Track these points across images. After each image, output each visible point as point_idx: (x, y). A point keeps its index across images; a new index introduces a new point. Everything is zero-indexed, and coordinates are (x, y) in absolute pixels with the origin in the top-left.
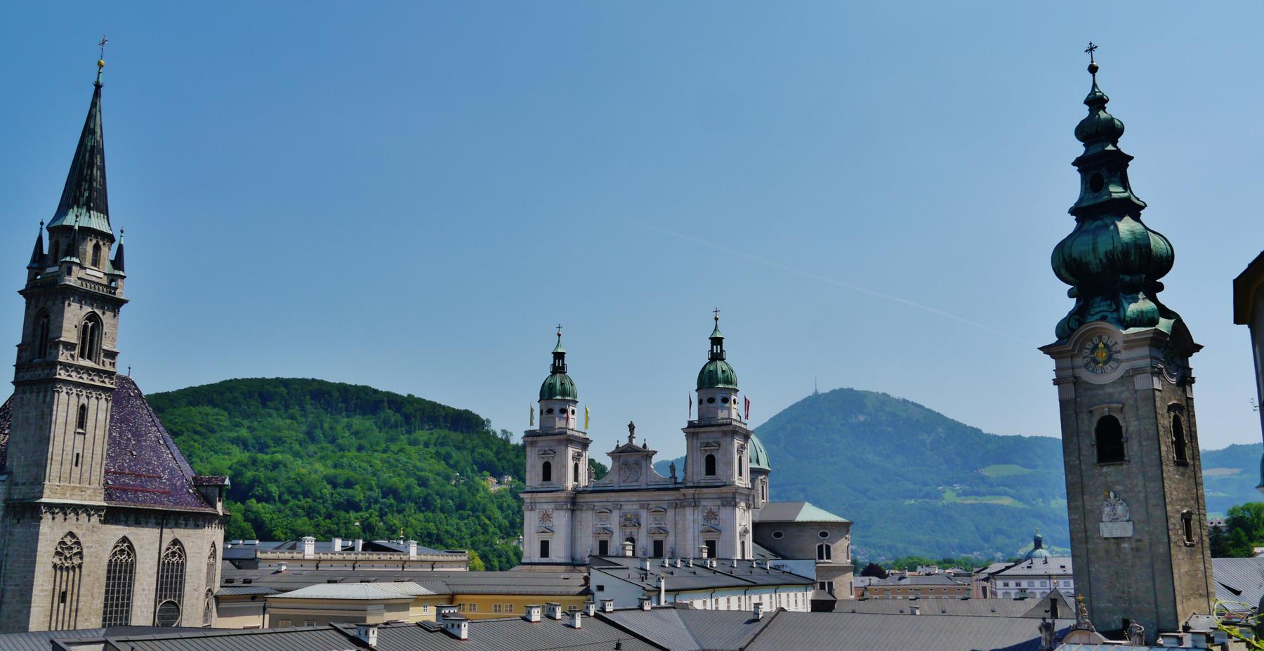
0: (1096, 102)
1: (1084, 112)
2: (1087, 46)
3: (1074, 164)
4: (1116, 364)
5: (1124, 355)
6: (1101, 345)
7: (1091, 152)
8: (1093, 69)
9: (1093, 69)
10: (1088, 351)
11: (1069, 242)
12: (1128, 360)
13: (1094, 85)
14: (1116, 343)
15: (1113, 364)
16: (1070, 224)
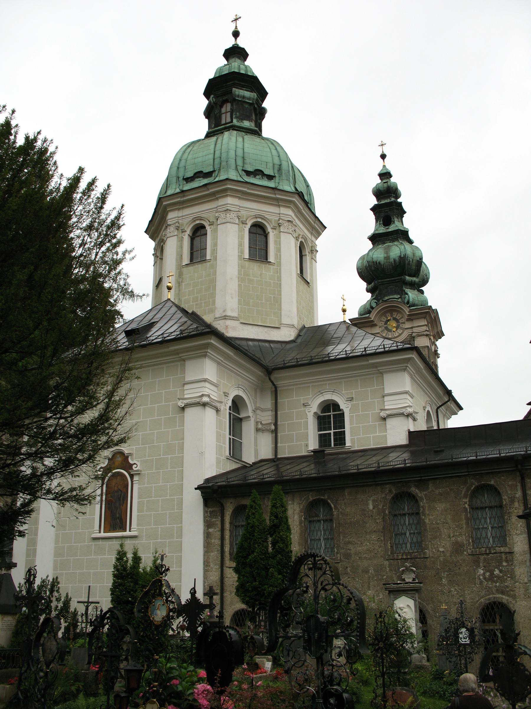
0: (385, 175)
1: (378, 181)
2: (380, 143)
3: (371, 209)
4: (402, 331)
5: (408, 325)
6: (392, 319)
7: (383, 202)
8: (383, 157)
9: (383, 157)
10: (383, 323)
11: (371, 254)
12: (412, 328)
13: (384, 166)
14: (402, 317)
15: (400, 331)
16: (369, 245)
